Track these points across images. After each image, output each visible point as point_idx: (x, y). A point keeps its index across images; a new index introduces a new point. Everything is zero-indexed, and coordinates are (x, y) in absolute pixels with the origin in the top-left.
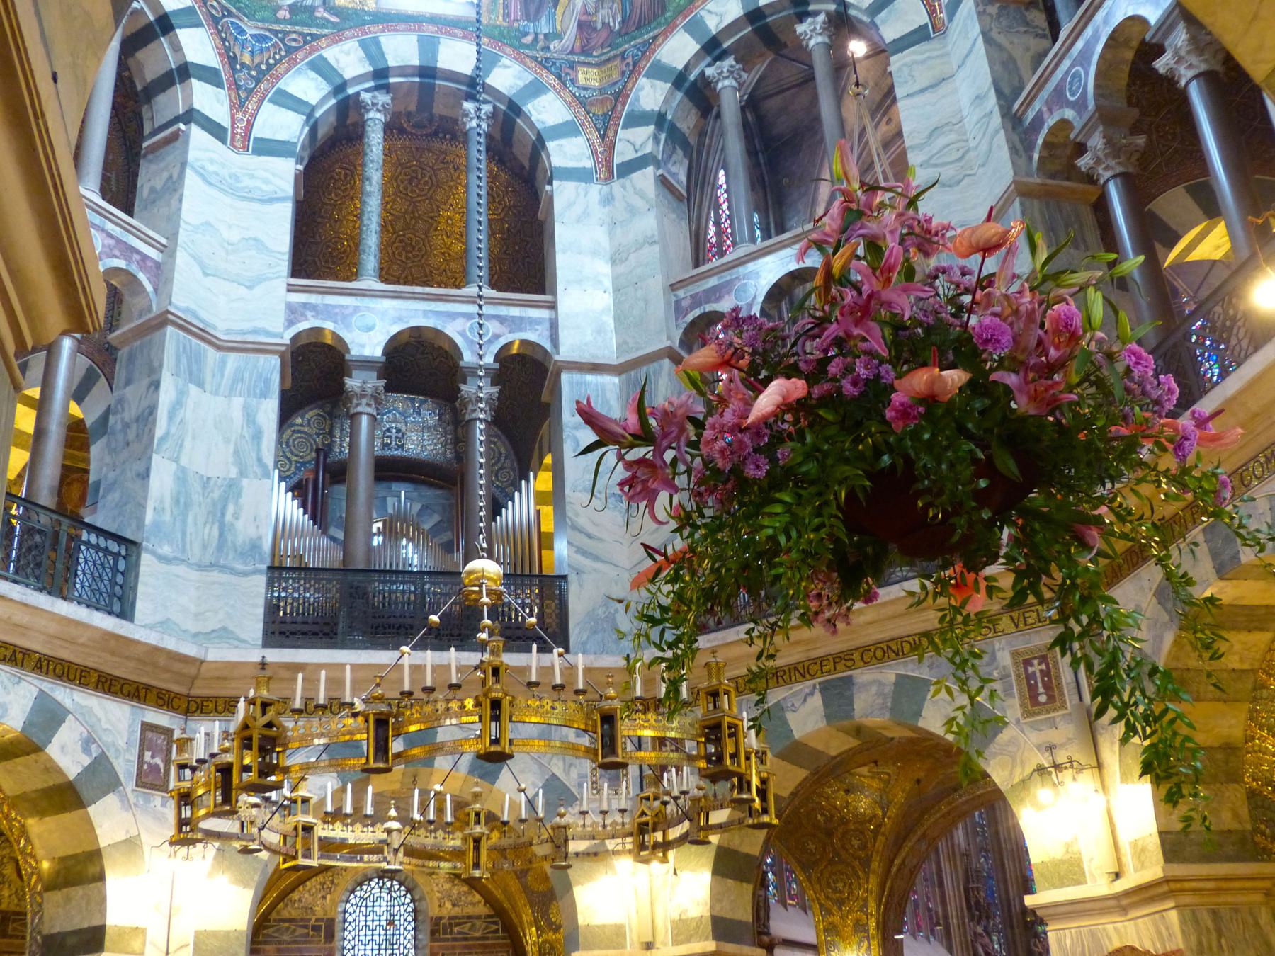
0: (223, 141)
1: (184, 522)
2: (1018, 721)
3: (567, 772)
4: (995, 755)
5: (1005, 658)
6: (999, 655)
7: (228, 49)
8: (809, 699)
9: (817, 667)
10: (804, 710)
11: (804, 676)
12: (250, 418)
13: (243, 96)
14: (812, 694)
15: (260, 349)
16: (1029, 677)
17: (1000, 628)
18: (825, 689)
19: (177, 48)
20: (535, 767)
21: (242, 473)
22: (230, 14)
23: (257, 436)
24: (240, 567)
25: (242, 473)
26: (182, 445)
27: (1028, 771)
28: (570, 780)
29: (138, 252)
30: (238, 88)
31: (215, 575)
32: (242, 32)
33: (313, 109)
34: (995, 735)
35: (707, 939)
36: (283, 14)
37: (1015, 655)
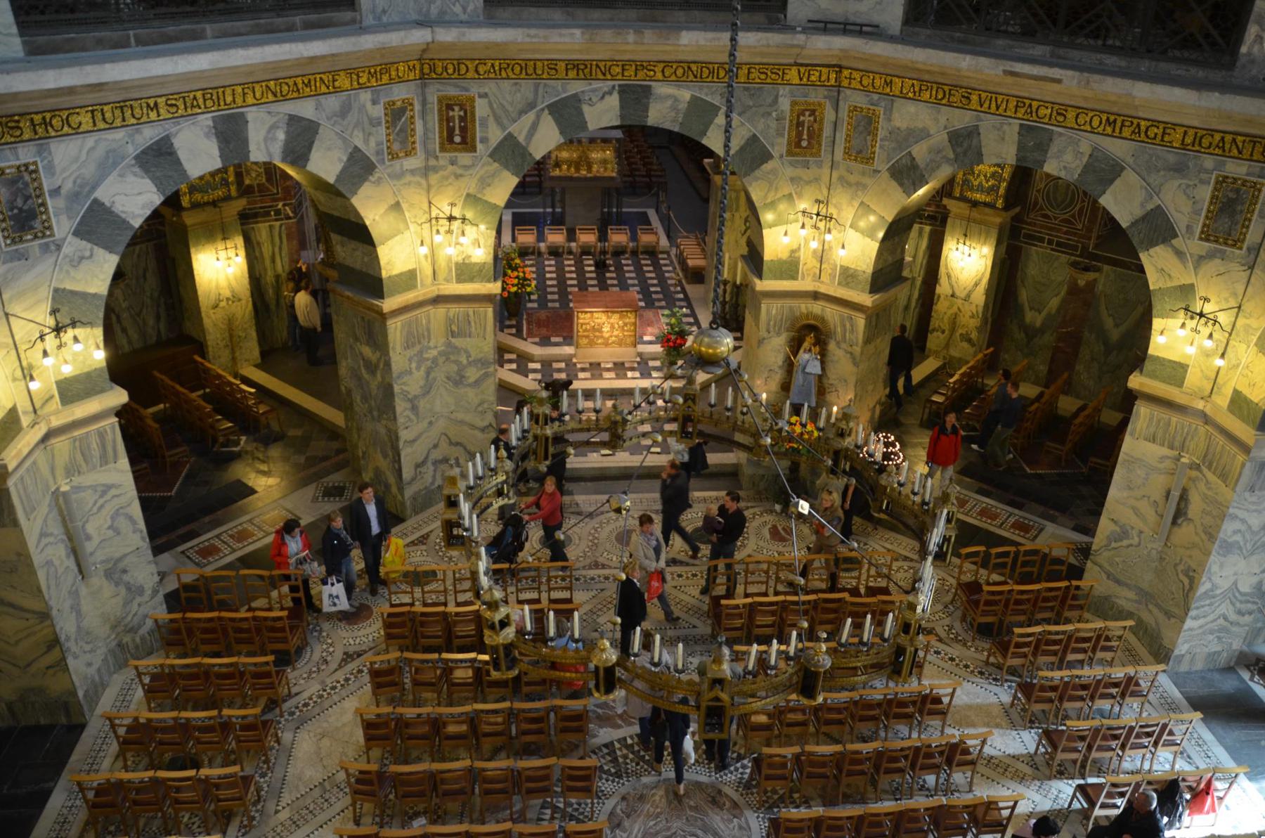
2: (781, 156)
3: (366, 141)
4: (757, 179)
5: (785, 104)
6: (780, 99)
8: (607, 97)
9: (618, 70)
10: (598, 105)
11: (604, 74)
14: (610, 93)
16: (800, 124)
17: (787, 77)
18: (623, 91)
20: (339, 142)
27: (779, 195)
28: (369, 150)
34: (762, 163)
35: (489, 281)
37: (794, 104)
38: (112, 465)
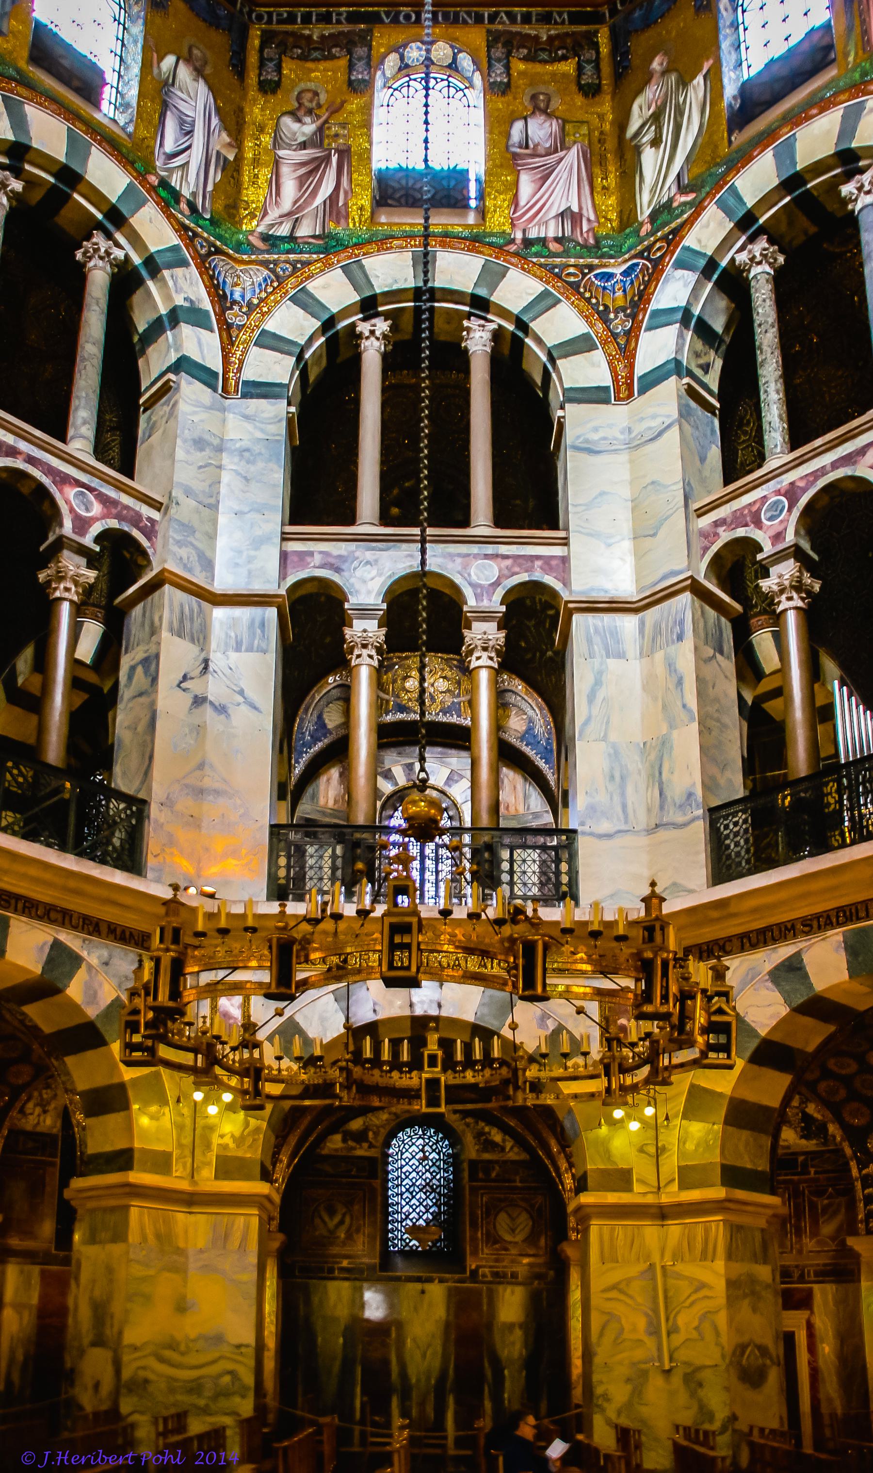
0: (607, 402)
1: (623, 794)
7: (595, 307)
12: (671, 666)
13: (622, 342)
15: (669, 594)
19: (539, 341)
21: (672, 726)
22: (591, 268)
23: (680, 682)
24: (680, 819)
25: (672, 726)
26: (608, 723)
29: (538, 557)
30: (615, 336)
31: (663, 834)
32: (611, 276)
33: (687, 313)
36: (643, 233)
38: (708, 1263)
